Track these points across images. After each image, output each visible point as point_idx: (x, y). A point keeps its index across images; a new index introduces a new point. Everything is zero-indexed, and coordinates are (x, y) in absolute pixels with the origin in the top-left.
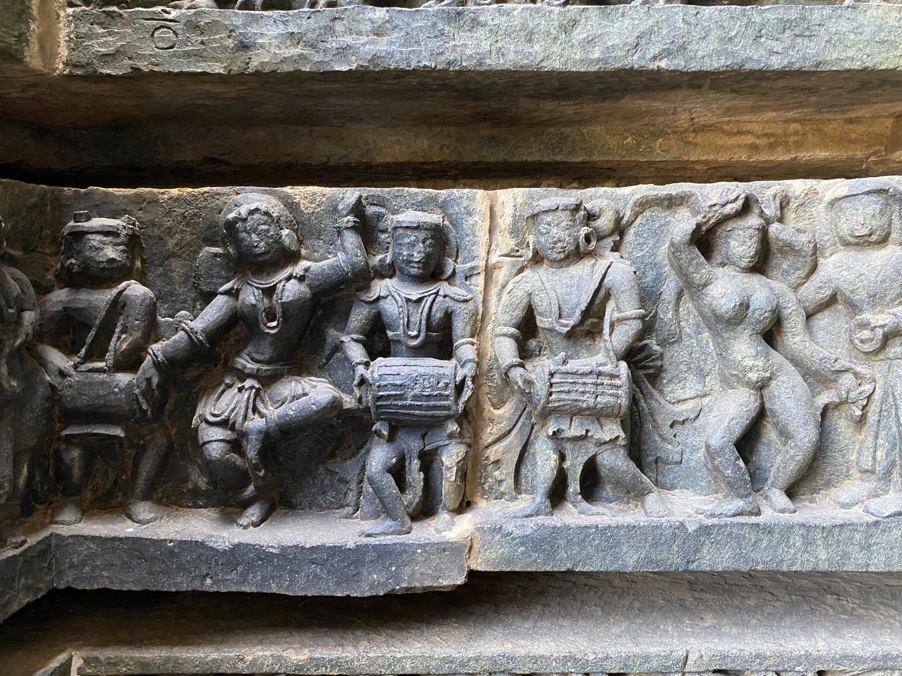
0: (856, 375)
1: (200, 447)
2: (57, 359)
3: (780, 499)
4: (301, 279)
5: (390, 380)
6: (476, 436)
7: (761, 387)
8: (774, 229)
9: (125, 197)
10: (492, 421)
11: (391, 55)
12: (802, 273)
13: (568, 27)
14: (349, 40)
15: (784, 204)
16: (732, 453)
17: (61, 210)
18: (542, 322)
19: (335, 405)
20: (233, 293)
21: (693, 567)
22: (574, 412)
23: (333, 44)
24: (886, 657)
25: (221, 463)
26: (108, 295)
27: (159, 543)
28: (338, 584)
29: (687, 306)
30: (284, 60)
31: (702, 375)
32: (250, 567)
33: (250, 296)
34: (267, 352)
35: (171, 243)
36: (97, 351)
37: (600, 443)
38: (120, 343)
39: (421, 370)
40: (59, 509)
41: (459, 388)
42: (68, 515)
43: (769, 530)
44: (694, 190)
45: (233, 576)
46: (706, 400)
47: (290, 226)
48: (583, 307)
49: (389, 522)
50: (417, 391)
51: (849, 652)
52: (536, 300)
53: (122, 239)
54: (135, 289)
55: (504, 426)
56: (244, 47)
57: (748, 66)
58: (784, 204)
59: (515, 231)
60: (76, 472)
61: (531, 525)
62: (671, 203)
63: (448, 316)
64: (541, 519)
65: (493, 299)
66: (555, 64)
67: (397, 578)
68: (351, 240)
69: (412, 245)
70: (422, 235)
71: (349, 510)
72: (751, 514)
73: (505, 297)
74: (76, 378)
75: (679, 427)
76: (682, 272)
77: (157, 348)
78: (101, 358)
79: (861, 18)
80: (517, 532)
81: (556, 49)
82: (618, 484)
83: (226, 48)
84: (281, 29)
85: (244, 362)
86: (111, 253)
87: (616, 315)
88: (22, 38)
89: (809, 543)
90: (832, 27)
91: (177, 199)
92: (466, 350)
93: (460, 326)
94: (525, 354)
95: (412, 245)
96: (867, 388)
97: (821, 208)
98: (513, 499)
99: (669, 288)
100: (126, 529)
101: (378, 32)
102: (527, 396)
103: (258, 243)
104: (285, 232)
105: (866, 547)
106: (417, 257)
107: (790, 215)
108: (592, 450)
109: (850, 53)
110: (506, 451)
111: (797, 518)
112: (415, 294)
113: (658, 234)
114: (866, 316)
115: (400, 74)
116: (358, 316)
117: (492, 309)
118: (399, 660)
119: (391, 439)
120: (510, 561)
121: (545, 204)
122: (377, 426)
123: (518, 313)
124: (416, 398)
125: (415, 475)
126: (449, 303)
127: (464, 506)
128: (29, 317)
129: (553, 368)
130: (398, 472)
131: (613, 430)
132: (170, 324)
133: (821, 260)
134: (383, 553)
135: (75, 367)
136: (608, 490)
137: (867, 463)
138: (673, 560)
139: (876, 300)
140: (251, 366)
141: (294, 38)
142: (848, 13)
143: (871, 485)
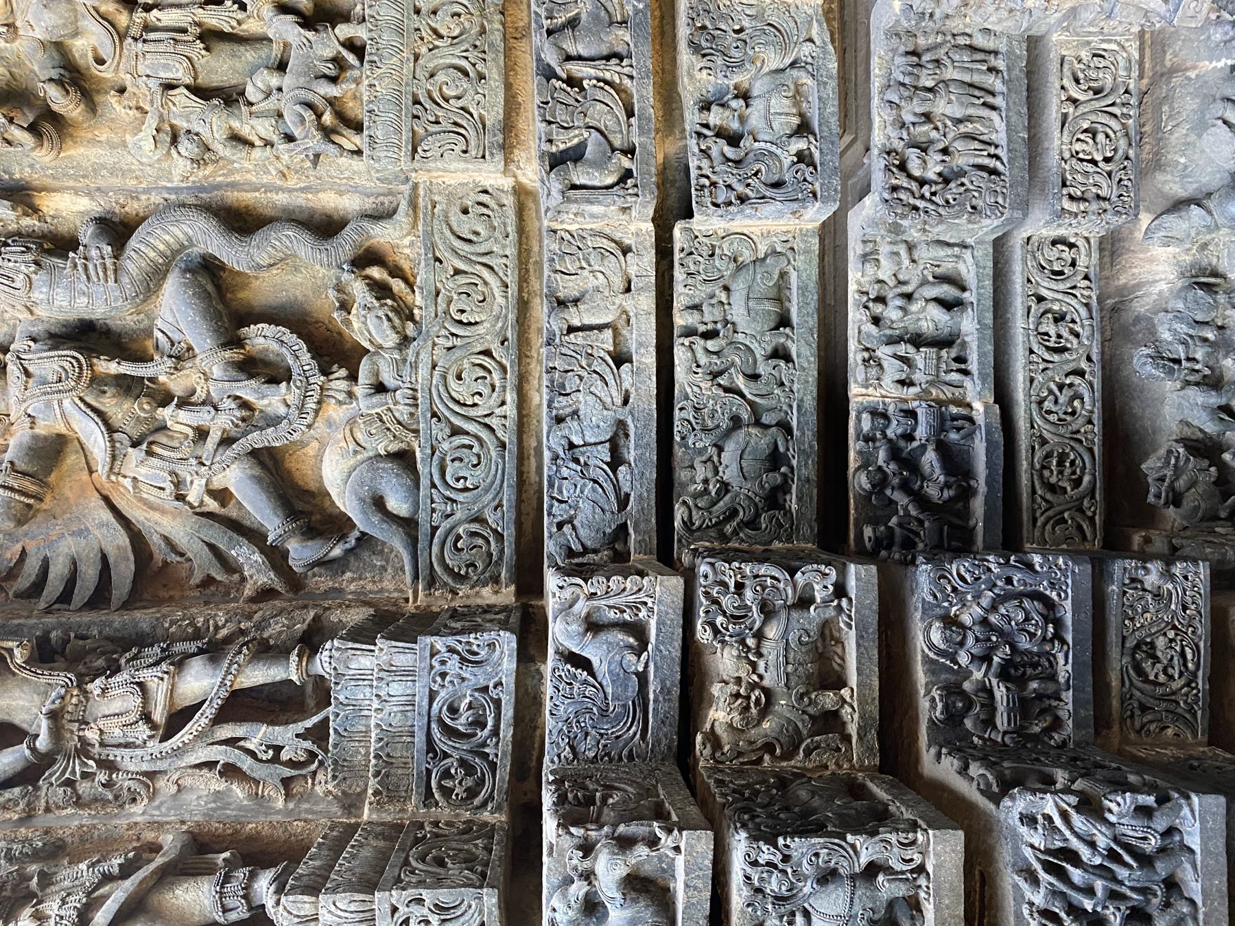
1: (951, 499)
3: (966, 295)
8: (872, 297)
16: (952, 313)
18: (904, 377)
19: (937, 450)
22: (938, 368)
26: (898, 530)
29: (894, 326)
31: (919, 319)
32: (993, 480)
33: (896, 481)
36: (917, 534)
38: (914, 526)
41: (930, 406)
43: (979, 300)
56: (808, 480)
59: (867, 388)
61: (977, 382)
63: (901, 411)
66: (816, 373)
68: (878, 444)
86: (882, 528)
91: (856, 510)
93: (905, 407)
99: (888, 332)
101: (804, 434)
102: (931, 383)
103: (879, 476)
105: (984, 268)
111: (974, 290)
113: (869, 335)
116: (902, 443)
125: (959, 423)
127: (969, 406)
130: (958, 429)
131: (944, 353)
134: (988, 433)
136: (962, 354)
138: (989, 332)
139: (899, 263)
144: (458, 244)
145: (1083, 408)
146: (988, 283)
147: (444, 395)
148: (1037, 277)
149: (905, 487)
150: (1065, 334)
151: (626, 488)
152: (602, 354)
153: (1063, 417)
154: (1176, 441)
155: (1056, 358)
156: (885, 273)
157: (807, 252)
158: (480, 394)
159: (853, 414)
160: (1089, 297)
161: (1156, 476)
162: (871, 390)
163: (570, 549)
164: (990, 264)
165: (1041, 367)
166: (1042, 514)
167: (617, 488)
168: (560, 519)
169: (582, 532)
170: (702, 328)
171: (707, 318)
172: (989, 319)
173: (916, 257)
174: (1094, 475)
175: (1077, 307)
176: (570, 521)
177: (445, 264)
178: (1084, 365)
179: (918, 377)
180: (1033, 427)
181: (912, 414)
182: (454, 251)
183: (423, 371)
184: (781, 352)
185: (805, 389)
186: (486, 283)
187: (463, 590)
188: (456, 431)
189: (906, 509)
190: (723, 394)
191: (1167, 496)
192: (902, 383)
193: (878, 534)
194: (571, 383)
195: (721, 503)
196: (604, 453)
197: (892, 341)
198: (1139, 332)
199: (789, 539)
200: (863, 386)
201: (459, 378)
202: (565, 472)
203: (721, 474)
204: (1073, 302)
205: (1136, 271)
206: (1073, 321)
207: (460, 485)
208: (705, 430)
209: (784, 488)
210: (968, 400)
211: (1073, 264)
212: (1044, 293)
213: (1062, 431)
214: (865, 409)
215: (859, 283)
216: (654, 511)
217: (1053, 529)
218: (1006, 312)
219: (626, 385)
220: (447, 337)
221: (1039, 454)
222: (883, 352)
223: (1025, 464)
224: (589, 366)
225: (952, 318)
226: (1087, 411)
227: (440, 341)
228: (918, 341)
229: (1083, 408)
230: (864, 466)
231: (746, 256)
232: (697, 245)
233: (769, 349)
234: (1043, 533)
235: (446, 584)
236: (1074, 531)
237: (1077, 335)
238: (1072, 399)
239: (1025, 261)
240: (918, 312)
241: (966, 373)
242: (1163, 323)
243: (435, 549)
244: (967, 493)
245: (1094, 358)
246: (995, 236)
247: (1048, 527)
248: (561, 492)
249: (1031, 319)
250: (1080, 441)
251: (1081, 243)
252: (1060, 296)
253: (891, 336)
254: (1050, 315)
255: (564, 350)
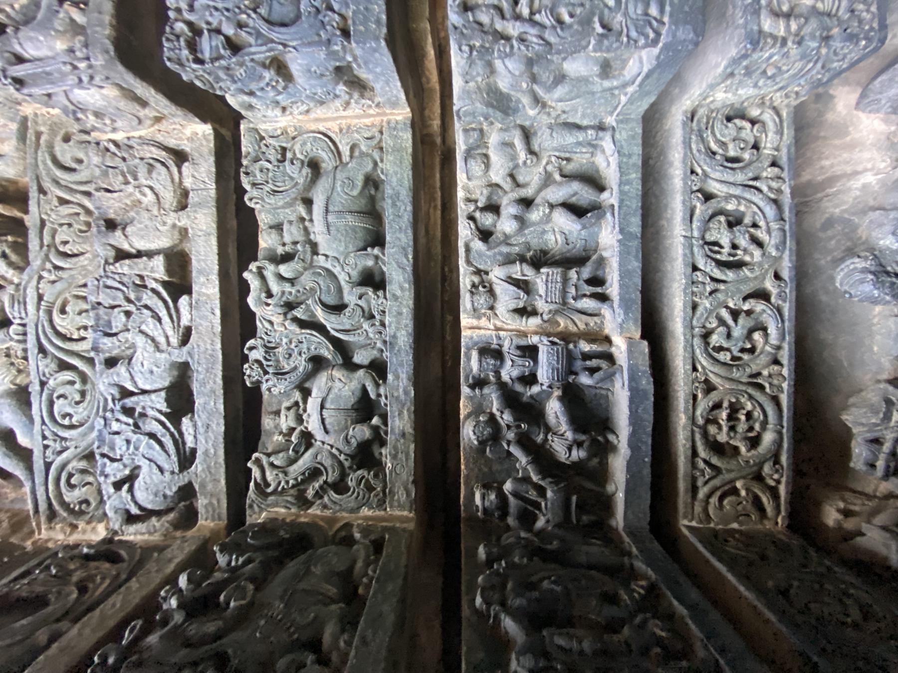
0: (547, 164)
2: (540, 523)
3: (605, 195)
4: (502, 412)
5: (550, 375)
6: (574, 334)
7: (552, 206)
8: (480, 205)
9: (465, 490)
10: (566, 327)
11: (407, 372)
12: (500, 191)
13: (395, 298)
14: (401, 390)
15: (469, 200)
16: (584, 220)
17: (472, 518)
18: (521, 305)
19: (561, 399)
20: (509, 443)
21: (639, 235)
22: (564, 292)
23: (403, 397)
24: (684, 142)
25: (588, 450)
26: (511, 499)
27: (628, 482)
28: (647, 399)
29: (513, 241)
30: (409, 417)
31: (544, 232)
33: (511, 435)
34: (535, 429)
35: (486, 470)
36: (537, 506)
37: (578, 279)
38: (532, 494)
39: (545, 360)
40: (610, 527)
41: (553, 343)
42: (613, 523)
43: (621, 201)
44: (463, 241)
45: (643, 448)
46: (556, 230)
47: (477, 416)
48: (515, 289)
49: (617, 375)
50: (555, 363)
51: (681, 159)
52: (511, 309)
53: (485, 491)
54: (508, 486)
55: (569, 323)
56: (403, 435)
57: (411, 220)
58: (469, 200)
59: (479, 318)
60: (593, 518)
61: (618, 310)
62: (468, 250)
63: (519, 348)
64: (616, 304)
65: (509, 327)
67: (644, 372)
68: (486, 391)
69: (488, 364)
70: (483, 359)
71: (610, 394)
72: (613, 210)
73: (509, 322)
74: (549, 516)
75: (570, 241)
76: (499, 244)
77: (535, 478)
78: (540, 504)
79: (391, 172)
80: (622, 317)
81: (405, 303)
82: (597, 269)
83: (404, 443)
84: (397, 419)
85: (540, 438)
86: (493, 497)
87: (519, 273)
88: (404, 530)
89: (628, 182)
90: (394, 184)
92: (535, 339)
93: (523, 342)
94: (534, 313)
95: (488, 364)
96: (553, 159)
97: (470, 183)
98: (604, 317)
99: (505, 249)
100: (621, 495)
101: (397, 377)
102: (557, 312)
104: (481, 418)
105: (630, 156)
106: (492, 362)
107: (473, 197)
108: (582, 282)
109: (405, 175)
110: (581, 320)
111: (615, 188)
112: (509, 363)
113: (480, 254)
114: (521, 162)
115: (415, 369)
116: (519, 388)
117: (514, 327)
118: (685, 372)
119: (576, 374)
120: (636, 320)
121: (469, 305)
122: (570, 380)
123: (516, 316)
124: (558, 363)
125: (594, 363)
126: (512, 347)
127: (608, 340)
128: (523, 534)
129: (544, 301)
130: (592, 371)
131: (573, 274)
132: (523, 472)
133: (494, 182)
134: (632, 379)
135: (544, 515)
136: (600, 273)
137: (588, 155)
138: (636, 244)
139: (514, 157)
140: (541, 436)
141: (400, 414)
142: (389, 178)
143: (599, 153)
144: (59, 173)
145: (766, 342)
146: (635, 176)
147: (49, 331)
148: (703, 165)
149: (524, 442)
150: (743, 242)
151: (190, 442)
152: (154, 285)
153: (740, 355)
154: (890, 382)
155: (730, 275)
156: (498, 175)
157: (397, 150)
158: (85, 328)
159: (463, 350)
160: (779, 191)
161: (869, 436)
162: (483, 322)
163: (128, 512)
164: (638, 150)
165: (708, 289)
166: (706, 483)
167: (179, 443)
168: (112, 479)
169: (140, 495)
170: (280, 250)
171: (287, 239)
172: (635, 225)
173: (536, 148)
174: (780, 433)
175: (761, 204)
176: (131, 479)
177: (49, 196)
178: (769, 285)
179: (541, 305)
180: (695, 369)
181: (530, 352)
182: (56, 182)
183: (31, 308)
184: (377, 278)
185: (398, 323)
186: (88, 212)
187: (81, 525)
188: (64, 366)
189: (525, 469)
190: (298, 330)
191: (888, 467)
192: (523, 312)
193: (487, 504)
194: (118, 321)
195: (301, 462)
196: (159, 403)
197: (509, 261)
198: (831, 238)
199: (381, 504)
200: (474, 317)
201: (63, 311)
202: (115, 426)
203: (305, 424)
204: (757, 198)
205: (826, 163)
206: (755, 225)
207: (66, 422)
208: (280, 374)
209: (379, 438)
210: (607, 331)
211: (756, 147)
212: (714, 187)
213: (736, 374)
214: (476, 344)
215: (467, 189)
216: (223, 470)
217: (721, 499)
218: (659, 217)
219: (185, 321)
220: (50, 271)
221: (703, 404)
222: (497, 274)
223: (681, 420)
224: (139, 299)
225: (584, 227)
226: (772, 346)
227: (45, 274)
228: (539, 260)
229: (766, 342)
230: (478, 410)
231: (327, 162)
232: (264, 149)
233: (355, 274)
234: (705, 510)
235: (64, 519)
236: (749, 507)
237: (759, 244)
238: (751, 331)
239: (687, 144)
240: (541, 222)
241: (603, 298)
242: (881, 225)
243: (51, 487)
244: (603, 449)
245: (786, 274)
246: (645, 105)
247: (714, 500)
248: (112, 448)
249: (696, 224)
250: (761, 387)
251: (768, 117)
252: (737, 191)
253: (508, 254)
254: (722, 219)
255: (110, 282)
